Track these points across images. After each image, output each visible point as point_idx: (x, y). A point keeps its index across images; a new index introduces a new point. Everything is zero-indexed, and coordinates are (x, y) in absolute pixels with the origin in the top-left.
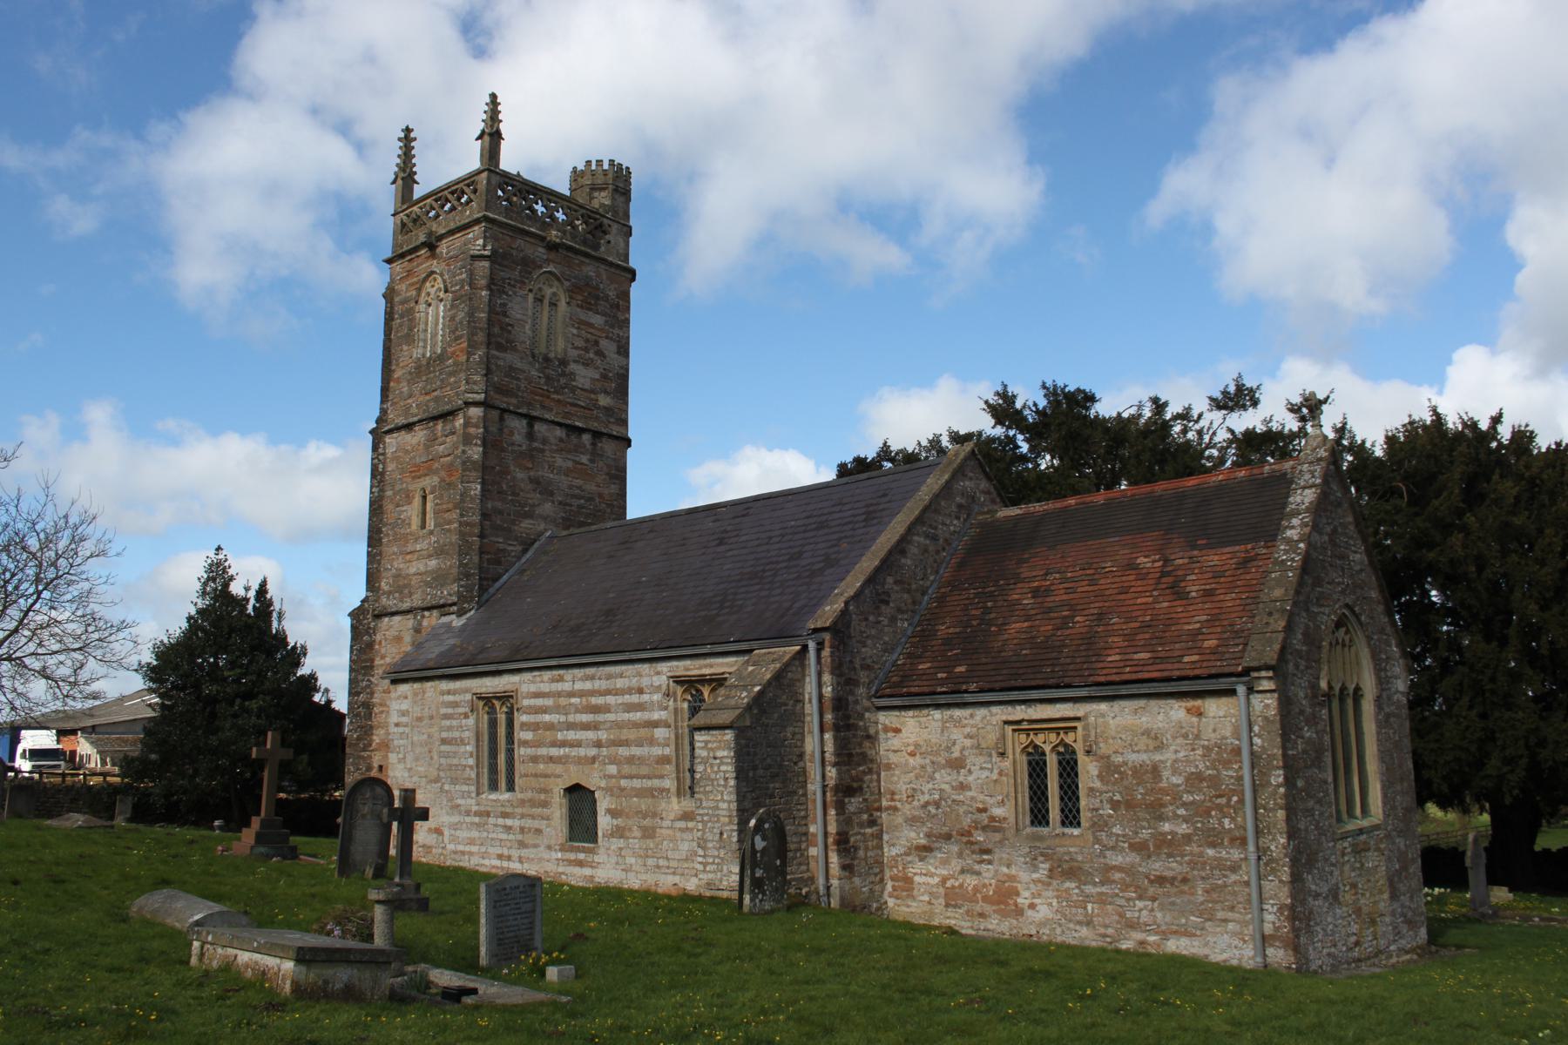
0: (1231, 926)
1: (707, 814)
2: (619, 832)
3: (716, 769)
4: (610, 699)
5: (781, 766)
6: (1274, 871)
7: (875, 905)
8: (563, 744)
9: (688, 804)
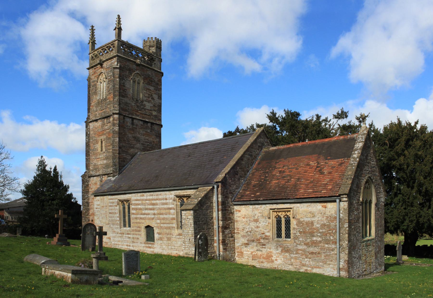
0: (331, 266)
1: (186, 234)
2: (161, 239)
3: (188, 221)
4: (158, 202)
5: (207, 221)
6: (344, 251)
7: (232, 259)
8: (144, 214)
9: (180, 231)
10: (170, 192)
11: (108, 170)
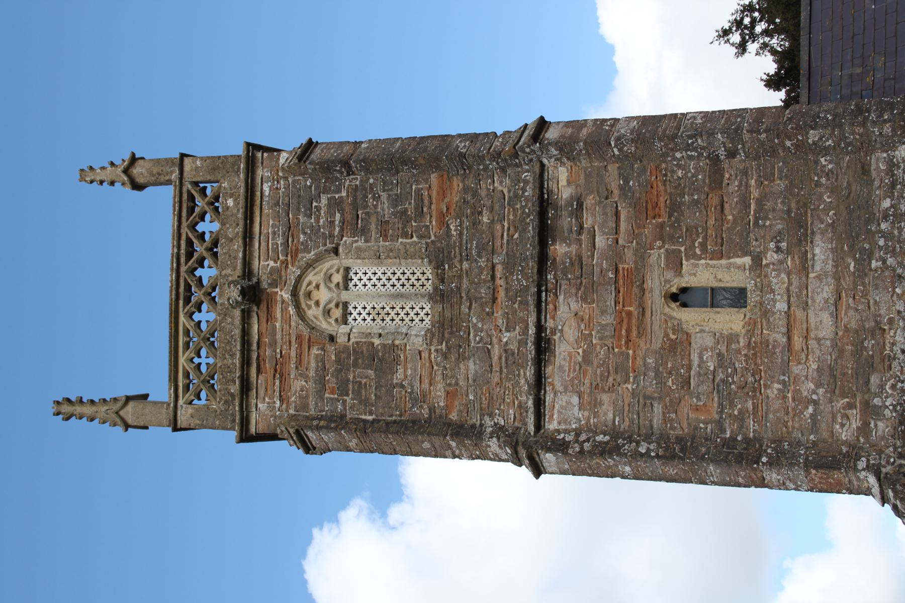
11: (886, 217)
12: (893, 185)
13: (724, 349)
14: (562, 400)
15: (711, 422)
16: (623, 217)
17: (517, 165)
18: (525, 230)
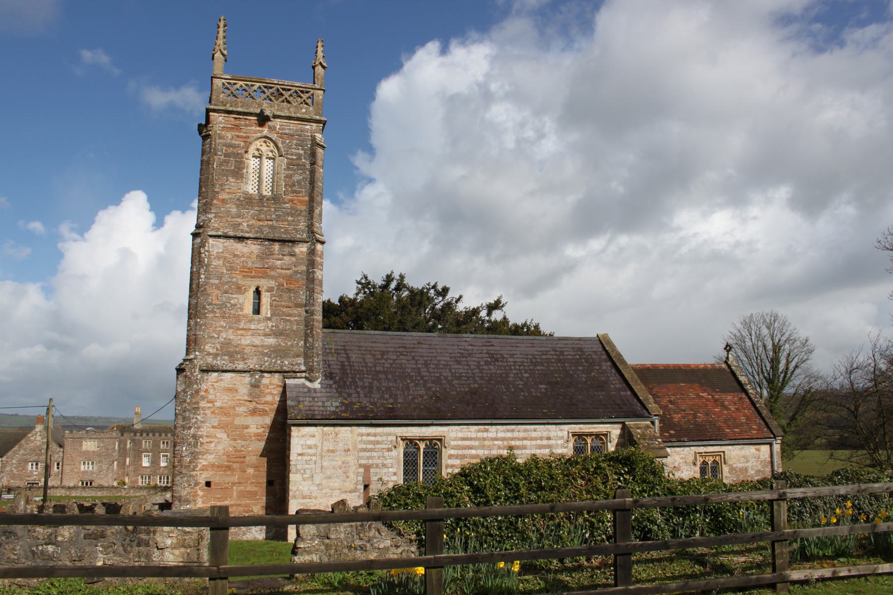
4: (525, 442)
10: (559, 426)
11: (282, 362)
12: (292, 365)
13: (238, 306)
14: (220, 245)
15: (212, 301)
16: (287, 271)
17: (308, 232)
18: (285, 234)
